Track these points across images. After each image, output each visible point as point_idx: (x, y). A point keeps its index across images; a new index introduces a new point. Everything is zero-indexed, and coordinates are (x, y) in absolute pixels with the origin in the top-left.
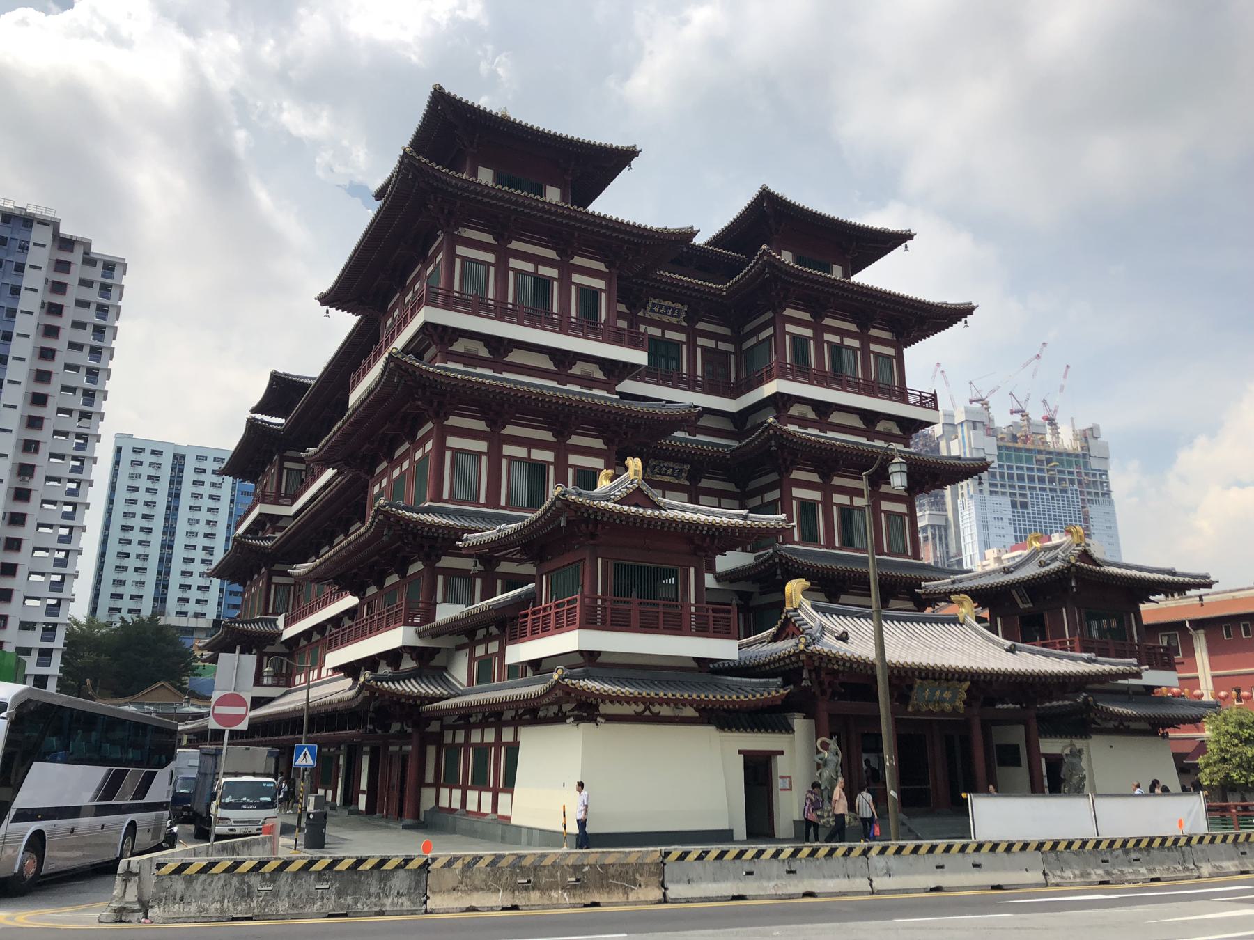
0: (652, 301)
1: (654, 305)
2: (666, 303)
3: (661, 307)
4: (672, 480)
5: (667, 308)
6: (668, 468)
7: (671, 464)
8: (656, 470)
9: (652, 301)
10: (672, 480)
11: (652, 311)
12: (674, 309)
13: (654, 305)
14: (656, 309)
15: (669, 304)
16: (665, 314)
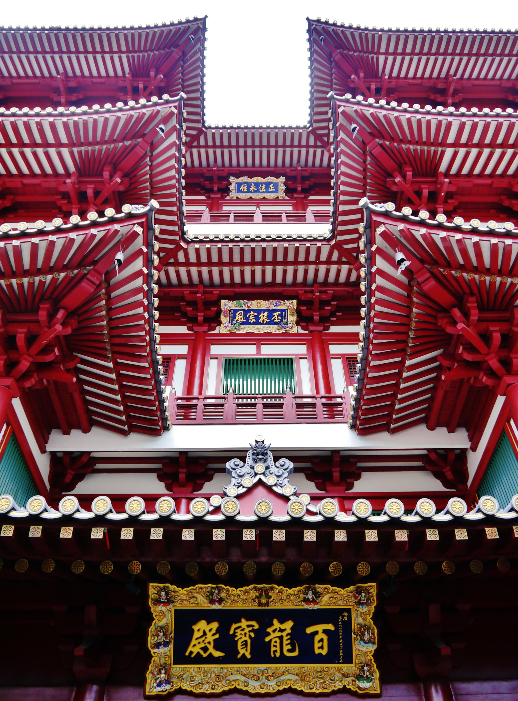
0: (232, 179)
1: (239, 185)
2: (255, 180)
3: (249, 185)
4: (273, 329)
5: (257, 185)
6: (259, 311)
7: (263, 304)
8: (239, 318)
9: (232, 179)
10: (273, 329)
11: (239, 191)
12: (268, 185)
13: (239, 185)
14: (244, 188)
15: (260, 180)
16: (255, 192)
